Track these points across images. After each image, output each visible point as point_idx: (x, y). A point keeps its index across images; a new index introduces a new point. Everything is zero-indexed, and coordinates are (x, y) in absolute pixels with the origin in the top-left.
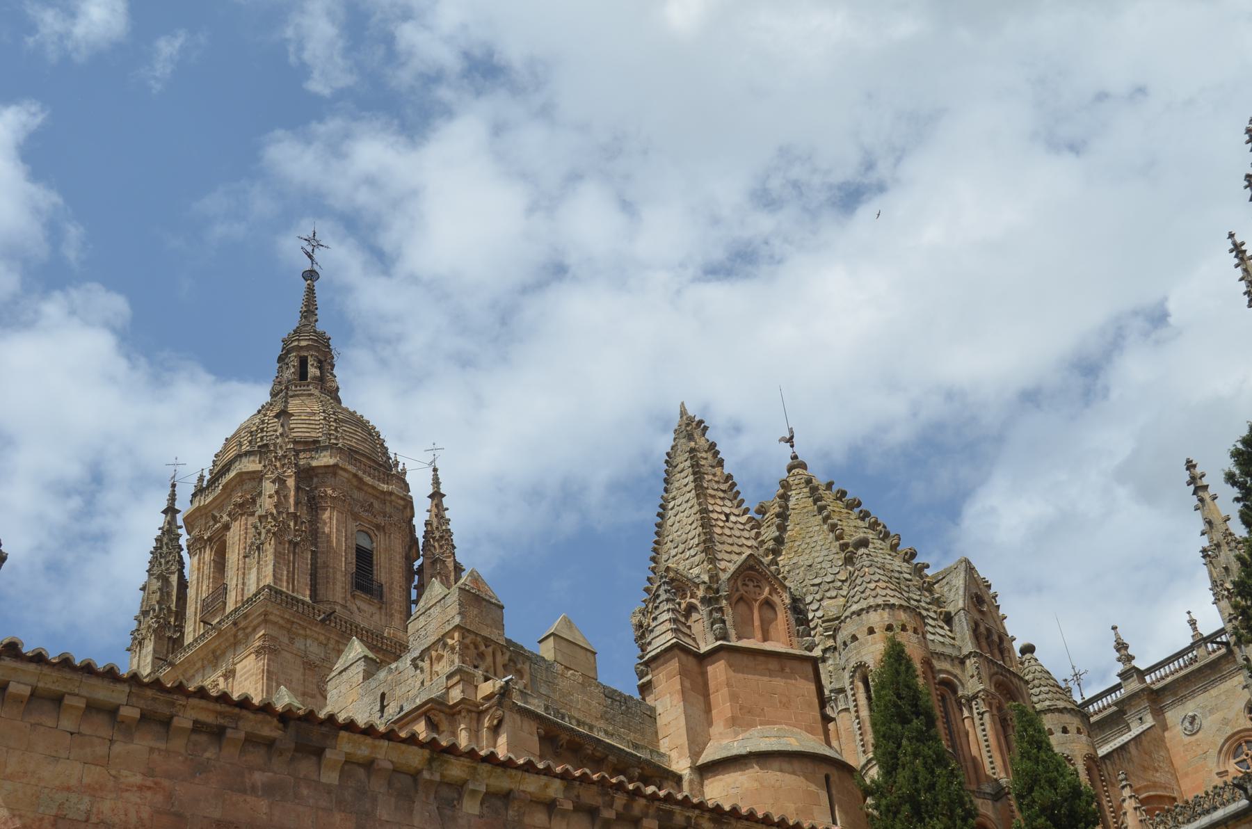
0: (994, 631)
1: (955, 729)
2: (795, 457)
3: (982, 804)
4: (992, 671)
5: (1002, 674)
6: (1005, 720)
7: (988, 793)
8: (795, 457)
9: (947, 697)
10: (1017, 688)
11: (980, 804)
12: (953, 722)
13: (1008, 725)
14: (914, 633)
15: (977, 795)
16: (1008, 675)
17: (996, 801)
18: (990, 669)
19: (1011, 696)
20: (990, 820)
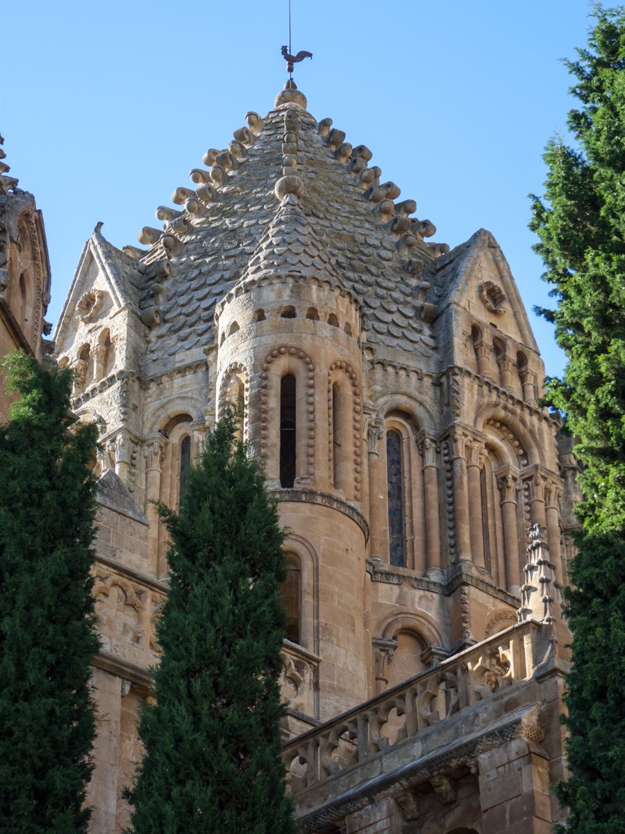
0: (509, 342)
1: (407, 485)
2: (291, 85)
3: (421, 598)
4: (486, 400)
5: (505, 408)
6: (504, 479)
7: (434, 584)
8: (291, 85)
9: (404, 436)
10: (532, 432)
11: (417, 599)
12: (406, 474)
13: (508, 487)
14: (330, 322)
15: (415, 584)
16: (519, 411)
17: (449, 595)
18: (481, 395)
19: (514, 435)
20: (430, 623)
